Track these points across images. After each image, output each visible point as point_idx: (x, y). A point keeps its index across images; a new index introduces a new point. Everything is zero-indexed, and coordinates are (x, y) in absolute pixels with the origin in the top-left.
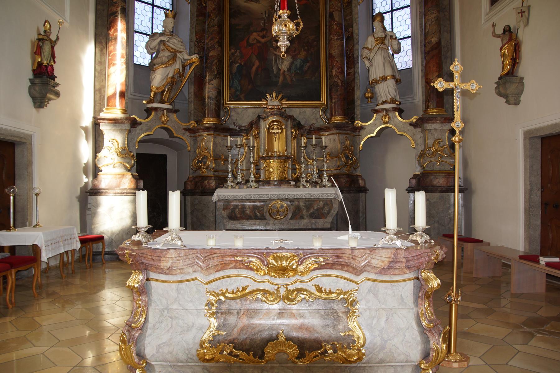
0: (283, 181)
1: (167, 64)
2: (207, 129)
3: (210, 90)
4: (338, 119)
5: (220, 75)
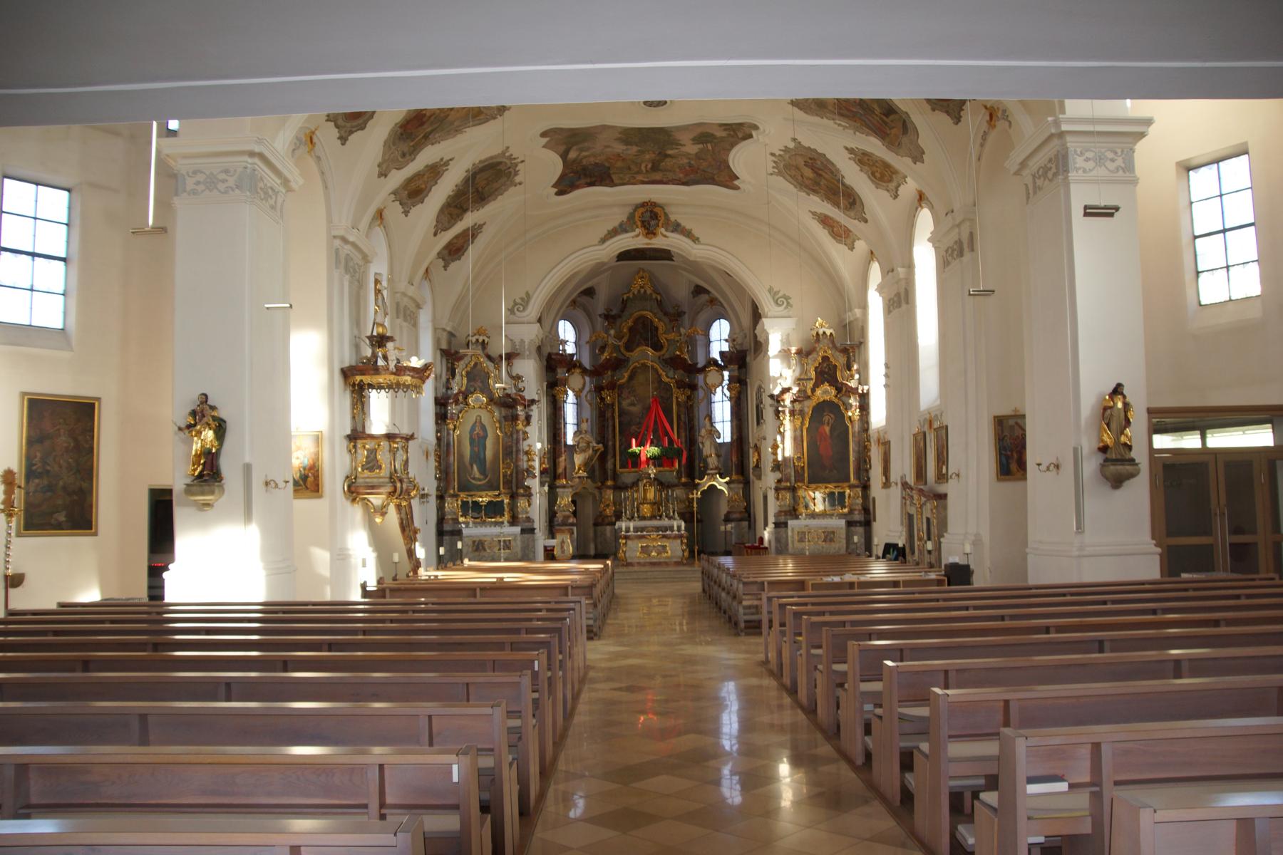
0: (653, 517)
1: (584, 451)
2: (609, 487)
3: (609, 465)
4: (683, 480)
5: (614, 456)
